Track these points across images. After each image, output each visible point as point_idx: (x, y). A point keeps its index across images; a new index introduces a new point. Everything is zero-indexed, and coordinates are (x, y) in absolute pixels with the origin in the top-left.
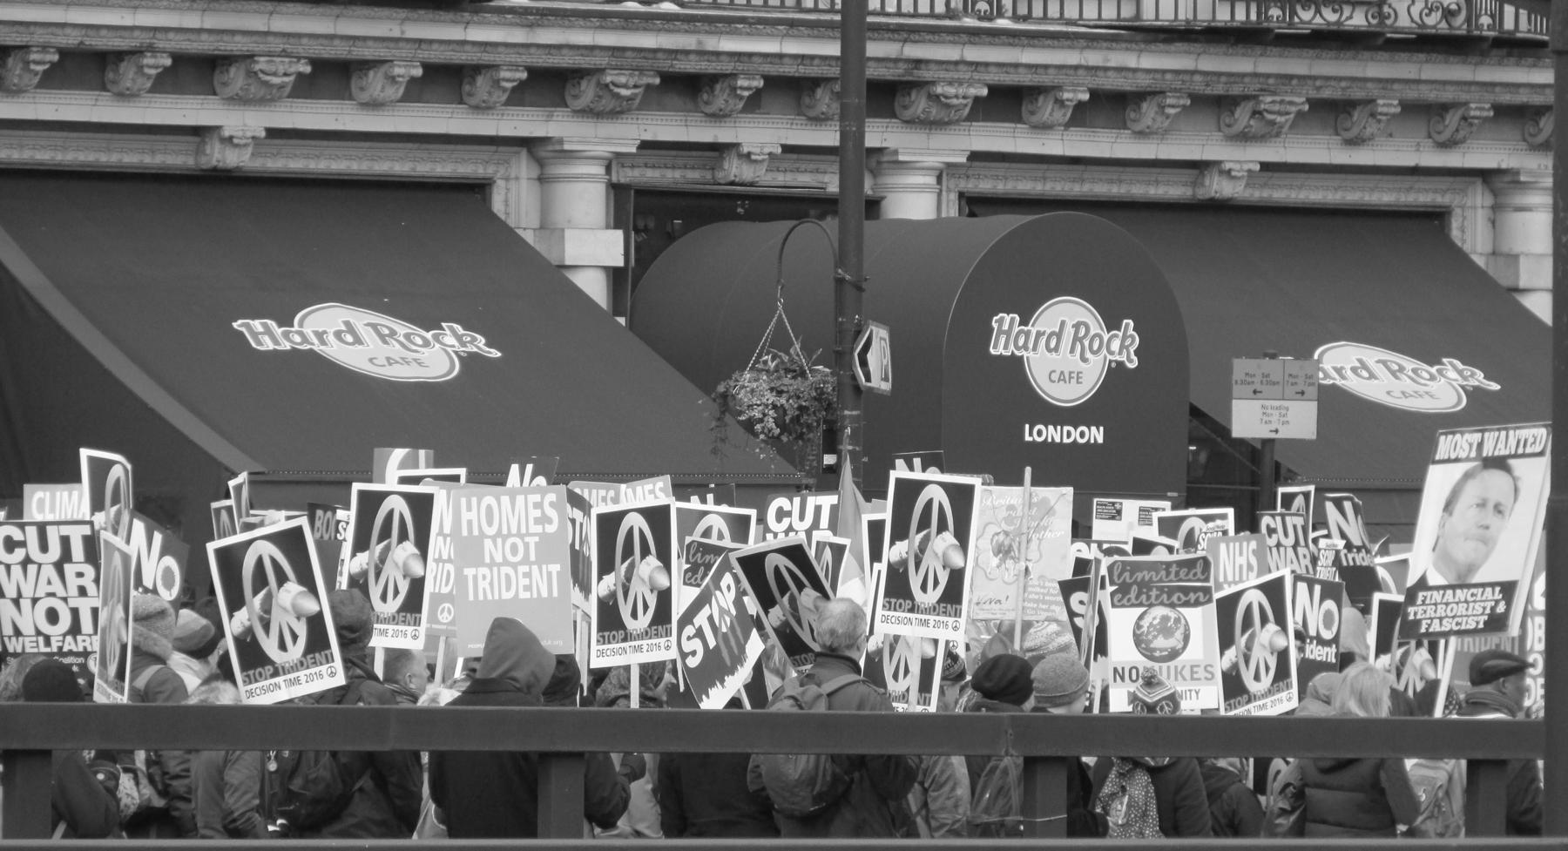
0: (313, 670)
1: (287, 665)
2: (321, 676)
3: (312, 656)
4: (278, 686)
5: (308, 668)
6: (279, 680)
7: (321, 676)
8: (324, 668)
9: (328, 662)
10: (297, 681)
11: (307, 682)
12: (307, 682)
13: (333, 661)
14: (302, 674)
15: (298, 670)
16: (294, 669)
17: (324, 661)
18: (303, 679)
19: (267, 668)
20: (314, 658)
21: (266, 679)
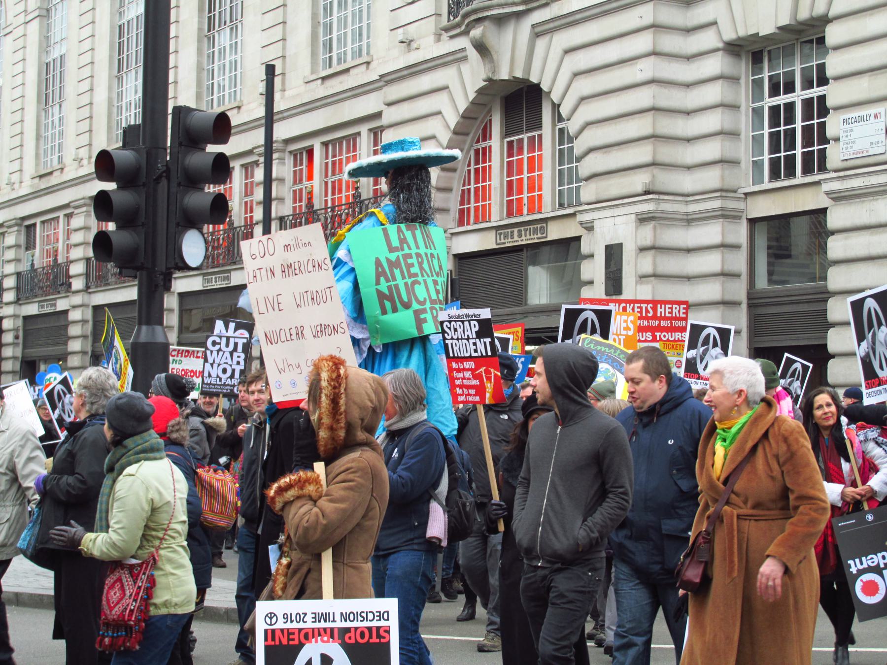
0: (295, 625)
1: (325, 639)
2: (285, 617)
3: (291, 643)
4: (345, 617)
5: (300, 630)
6: (340, 624)
7: (285, 617)
8: (280, 625)
9: (273, 631)
10: (317, 617)
11: (305, 614)
12: (305, 614)
13: (266, 631)
14: (309, 624)
15: (313, 629)
16: (320, 632)
17: (278, 634)
18: (309, 618)
19: (353, 641)
20: (289, 640)
21: (356, 629)
